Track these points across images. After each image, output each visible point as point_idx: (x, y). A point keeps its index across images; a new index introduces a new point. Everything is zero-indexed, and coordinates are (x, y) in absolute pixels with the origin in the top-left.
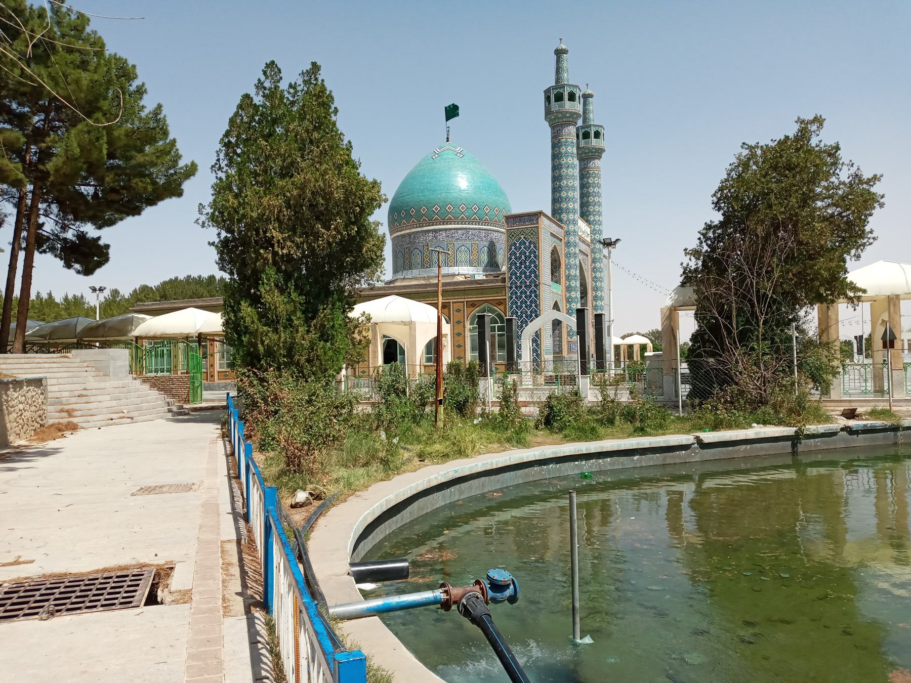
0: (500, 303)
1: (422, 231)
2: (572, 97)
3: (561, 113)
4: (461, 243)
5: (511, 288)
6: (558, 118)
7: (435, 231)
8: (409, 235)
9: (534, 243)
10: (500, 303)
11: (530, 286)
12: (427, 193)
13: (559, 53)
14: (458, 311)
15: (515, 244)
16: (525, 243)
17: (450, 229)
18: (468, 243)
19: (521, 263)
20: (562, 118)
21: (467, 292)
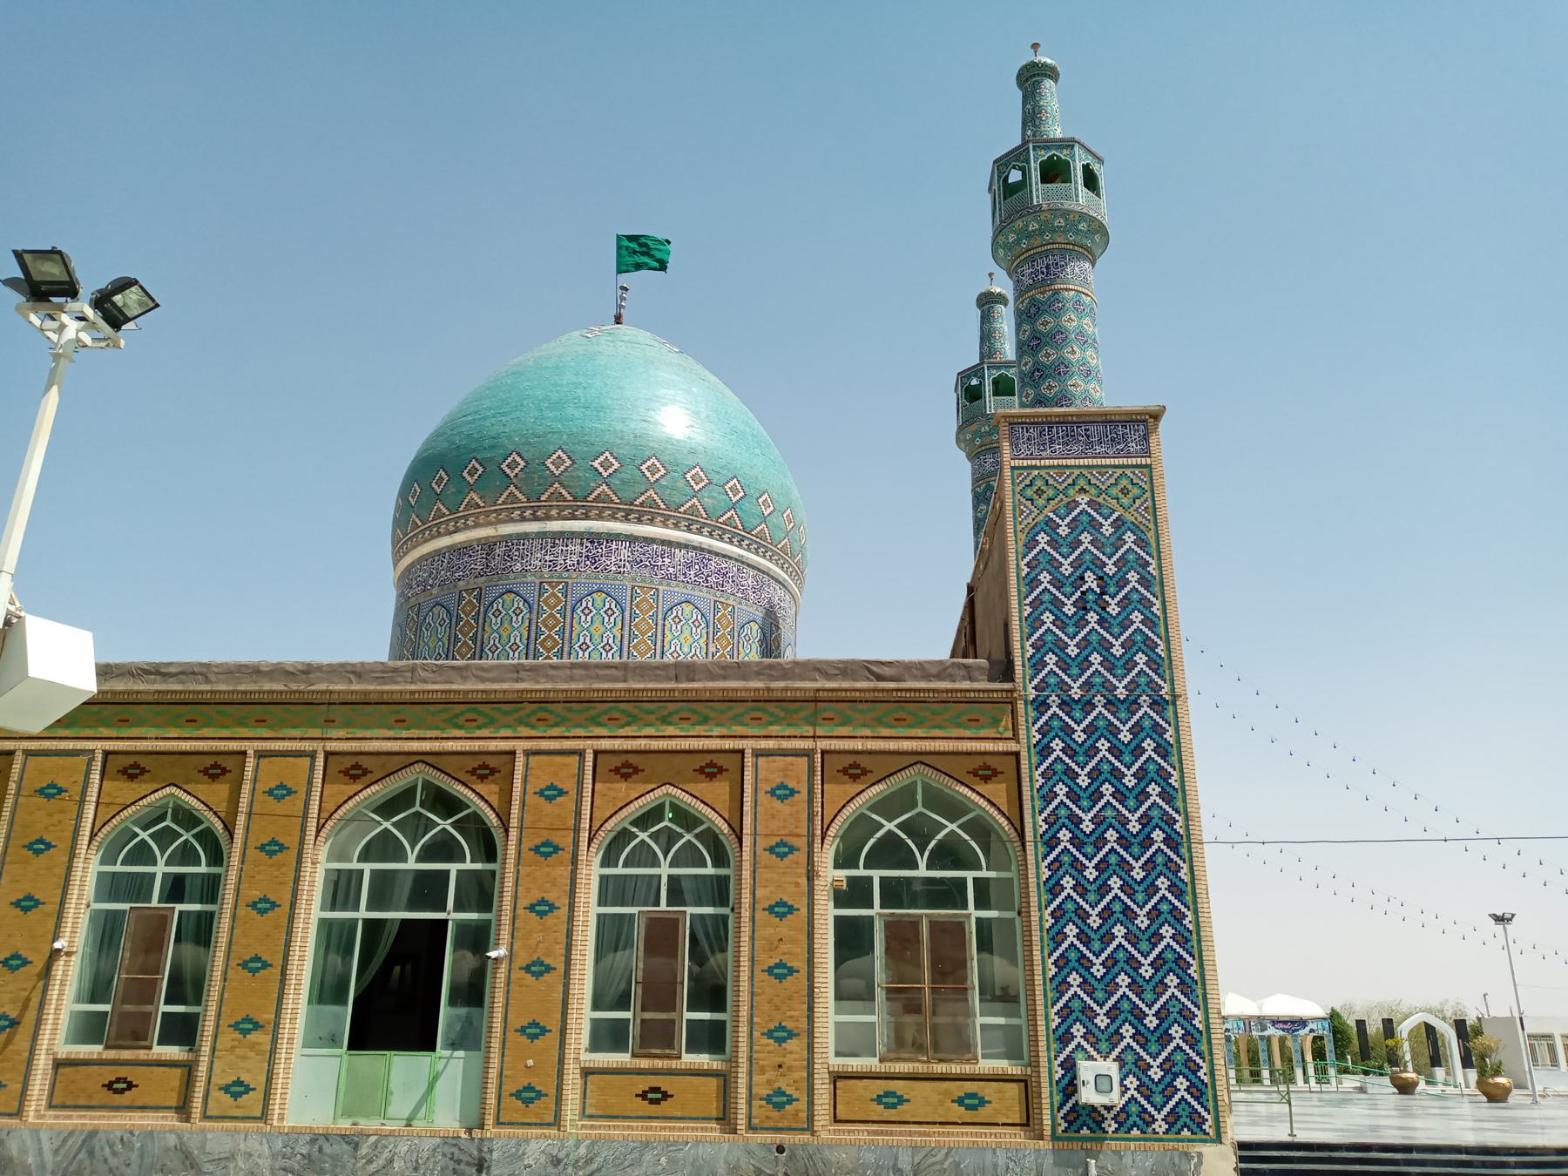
0: (985, 771)
1: (542, 535)
2: (1091, 181)
3: (1066, 214)
4: (680, 591)
5: (1041, 705)
6: (1053, 230)
7: (594, 538)
8: (489, 545)
9: (1135, 529)
10: (985, 771)
11: (1132, 704)
12: (571, 411)
13: (1032, 77)
14: (783, 792)
15: (1051, 526)
16: (1095, 526)
17: (649, 541)
18: (704, 596)
19: (1082, 605)
20: (1065, 231)
21: (829, 710)
